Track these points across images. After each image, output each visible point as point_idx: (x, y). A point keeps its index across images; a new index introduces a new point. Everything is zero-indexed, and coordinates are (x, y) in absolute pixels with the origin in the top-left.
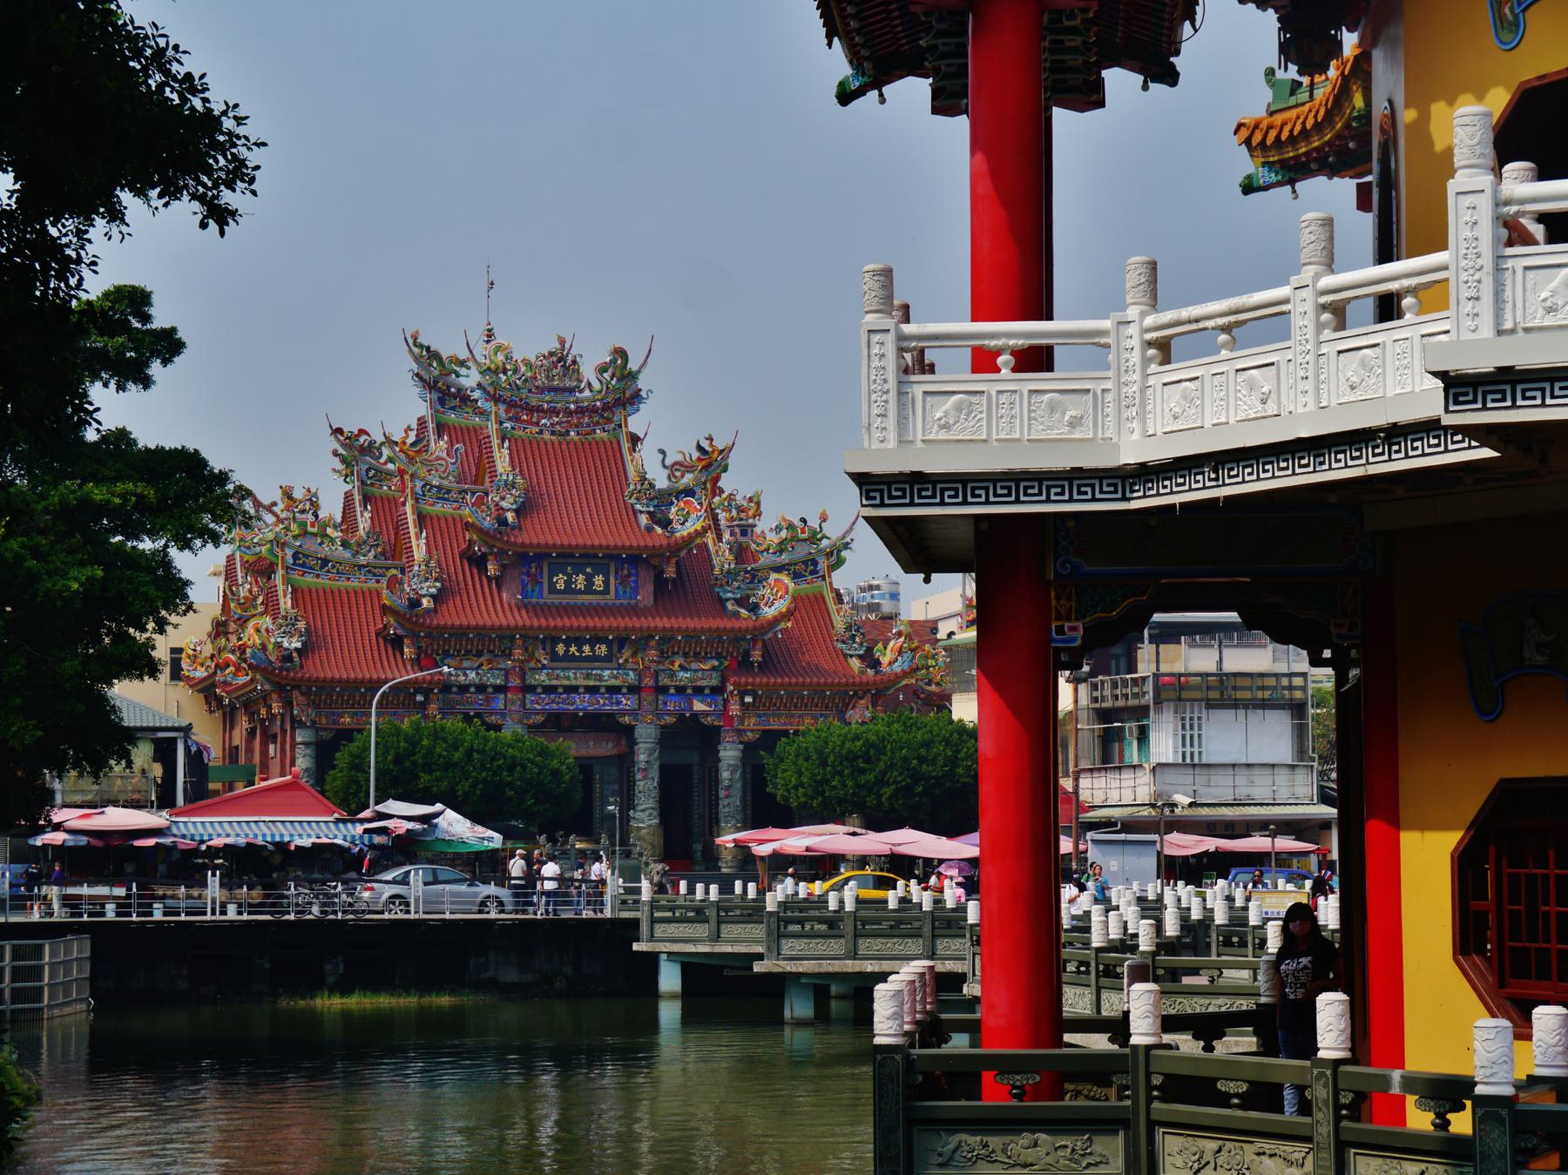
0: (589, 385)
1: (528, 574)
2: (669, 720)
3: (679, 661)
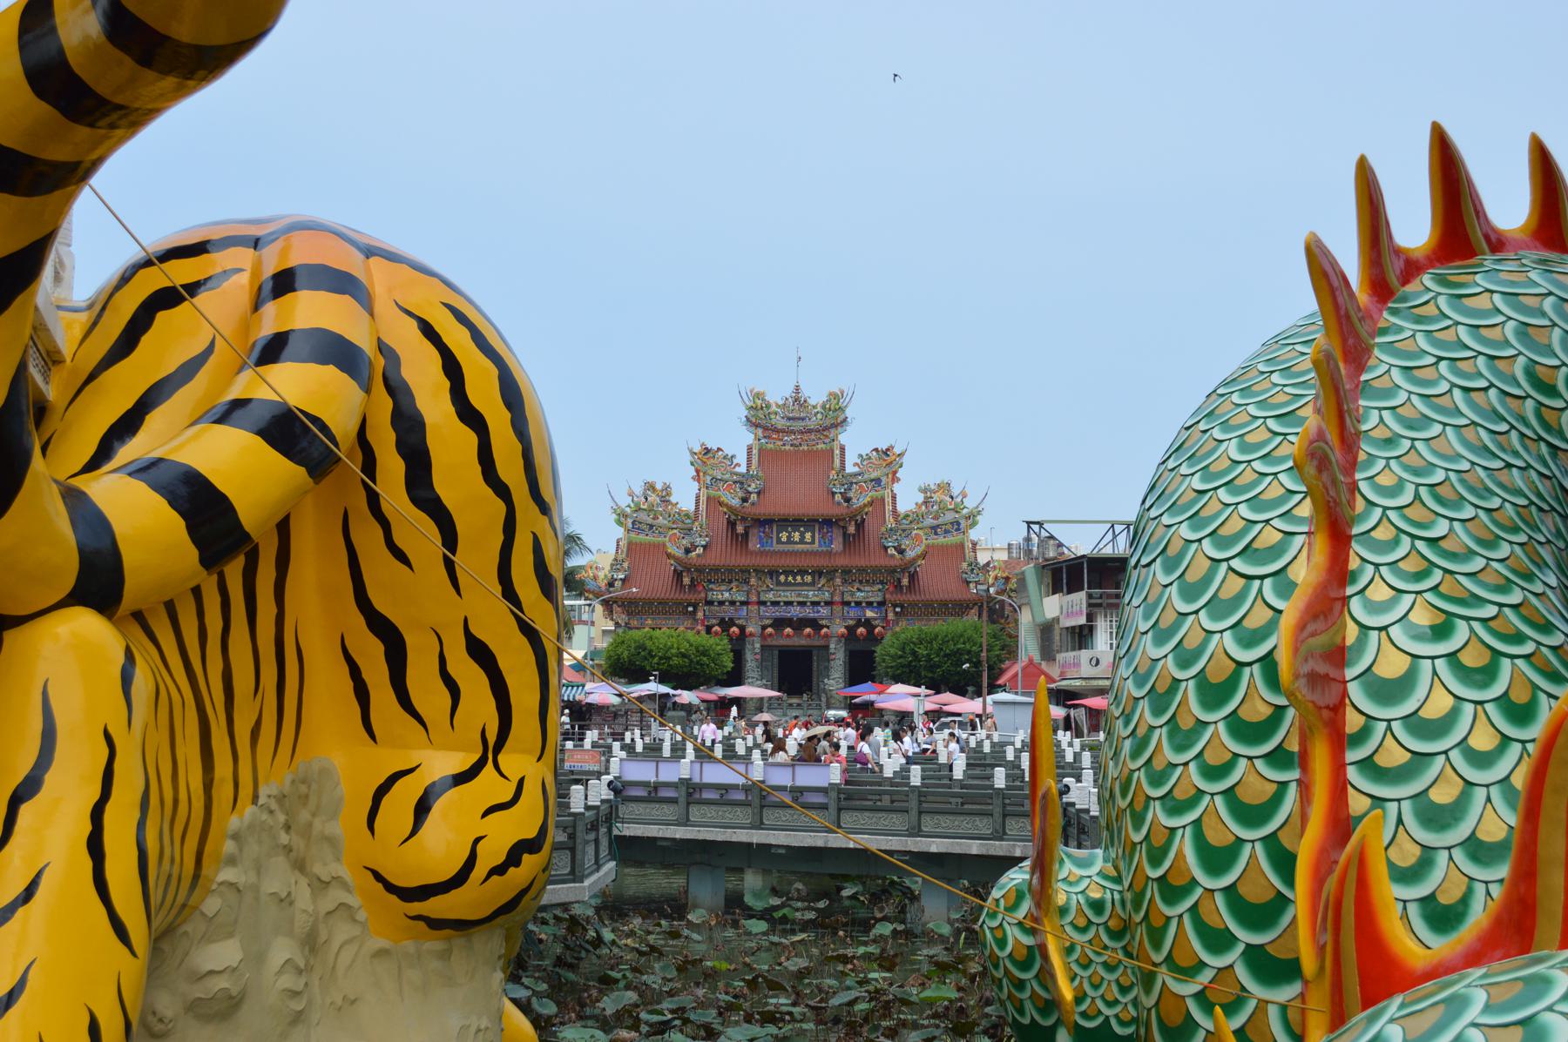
3: (857, 585)
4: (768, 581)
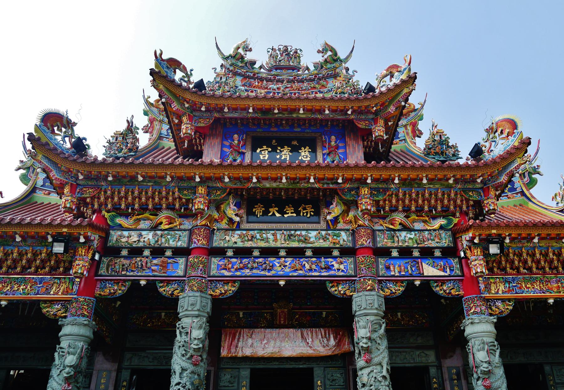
0: (308, 69)
1: (231, 146)
2: (398, 289)
4: (231, 211)
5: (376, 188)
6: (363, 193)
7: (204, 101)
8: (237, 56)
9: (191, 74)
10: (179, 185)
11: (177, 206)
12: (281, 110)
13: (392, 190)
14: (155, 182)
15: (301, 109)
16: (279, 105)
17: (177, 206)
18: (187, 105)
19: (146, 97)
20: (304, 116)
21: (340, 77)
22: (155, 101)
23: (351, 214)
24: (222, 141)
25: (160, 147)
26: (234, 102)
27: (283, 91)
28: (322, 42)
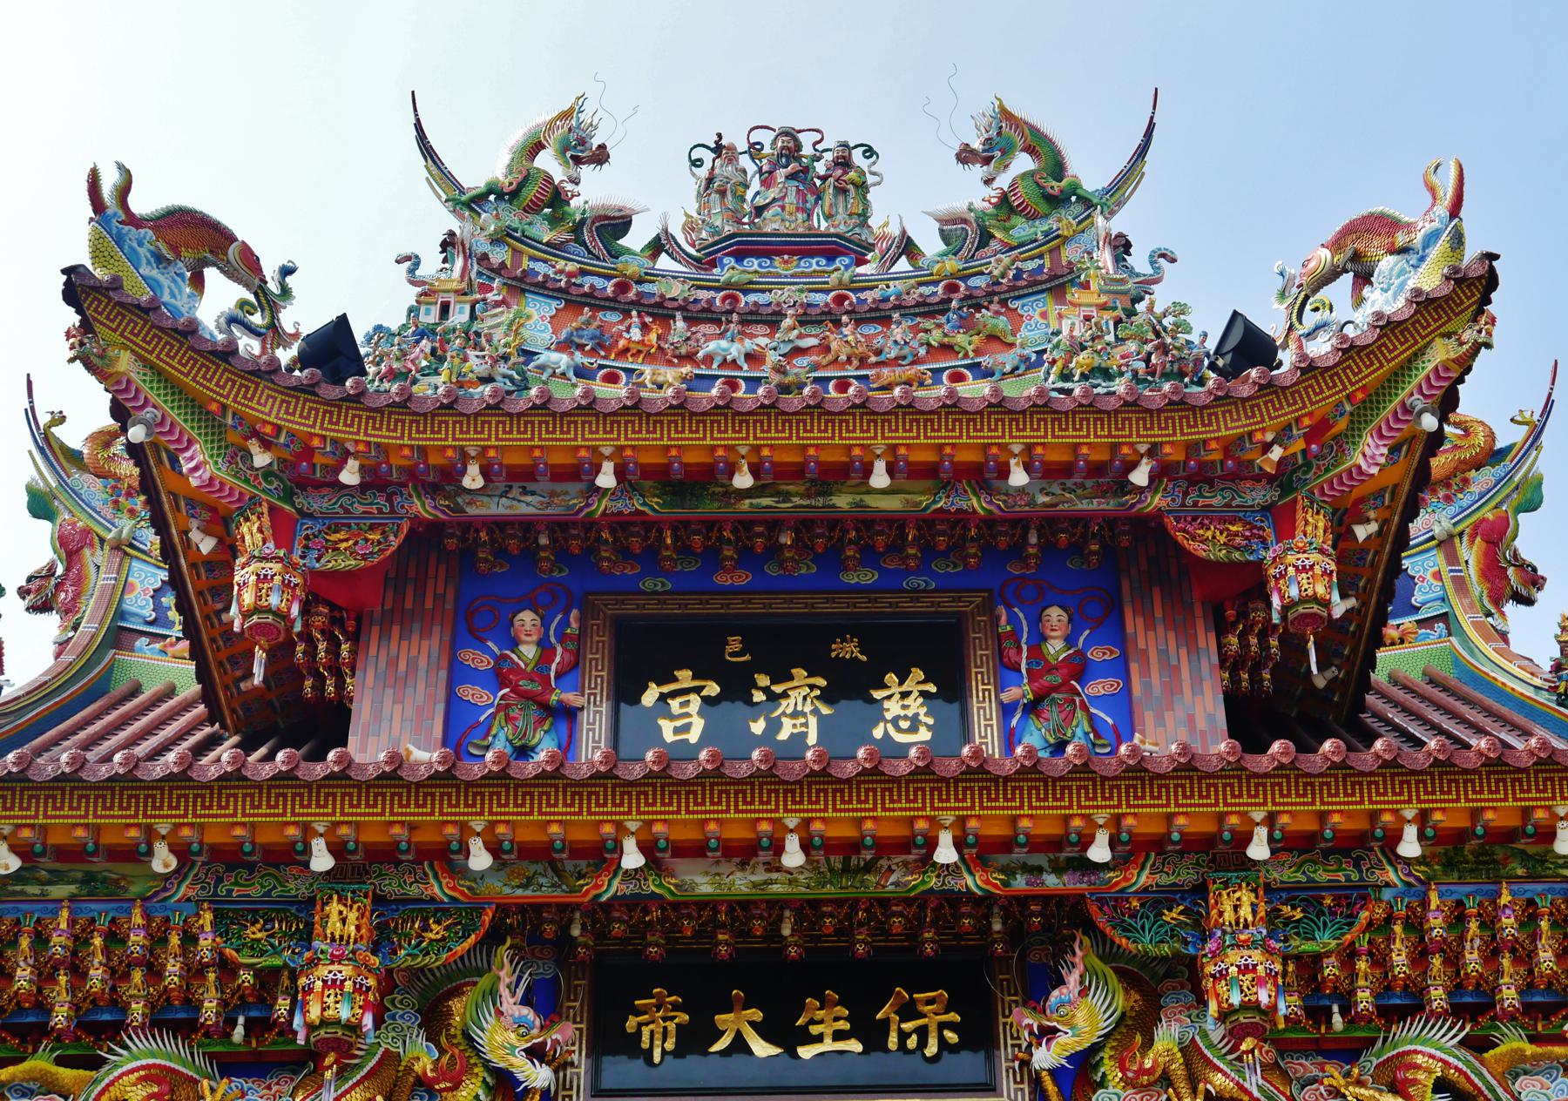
0: (908, 247)
1: (501, 675)
5: (1296, 887)
6: (1229, 916)
7: (352, 432)
8: (530, 193)
9: (286, 292)
10: (222, 891)
11: (210, 1009)
12: (770, 476)
13: (1387, 895)
14: (88, 879)
15: (880, 467)
16: (756, 449)
17: (210, 1009)
18: (261, 459)
19: (43, 419)
20: (893, 503)
21: (1086, 286)
22: (93, 438)
23: (1167, 1037)
24: (454, 646)
25: (119, 687)
26: (515, 438)
27: (779, 370)
28: (984, 106)
